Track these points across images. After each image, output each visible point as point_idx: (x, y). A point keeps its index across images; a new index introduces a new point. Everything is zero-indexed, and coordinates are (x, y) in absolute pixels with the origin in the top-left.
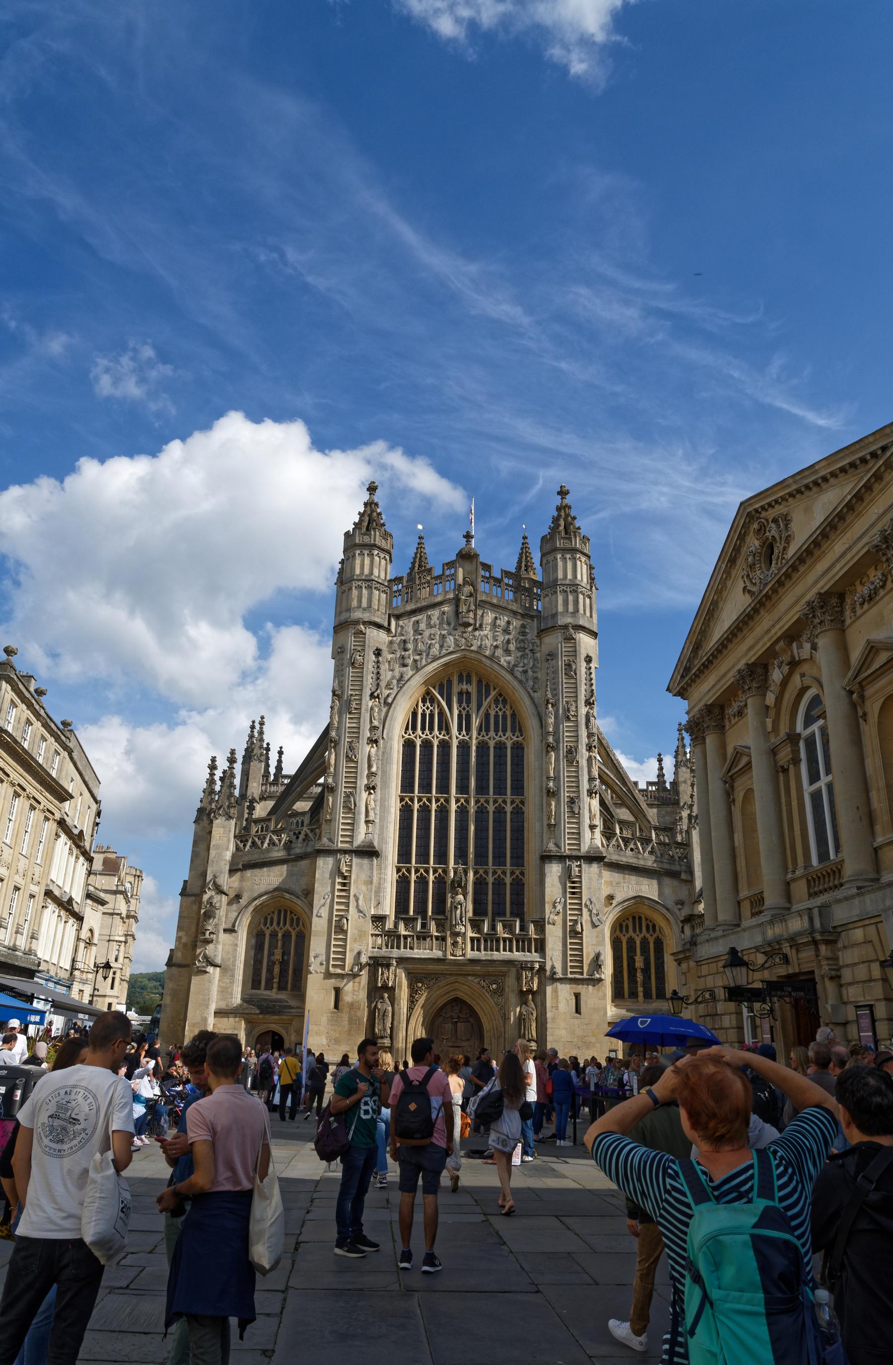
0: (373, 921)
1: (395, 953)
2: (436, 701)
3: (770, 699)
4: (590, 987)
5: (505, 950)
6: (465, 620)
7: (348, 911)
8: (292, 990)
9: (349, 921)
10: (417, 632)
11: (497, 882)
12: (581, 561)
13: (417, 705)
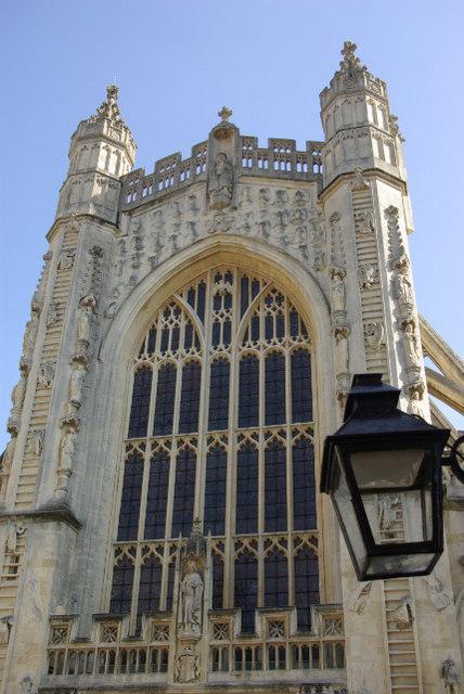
0: (54, 628)
5: (272, 667)
11: (273, 558)
12: (373, 105)
13: (157, 321)
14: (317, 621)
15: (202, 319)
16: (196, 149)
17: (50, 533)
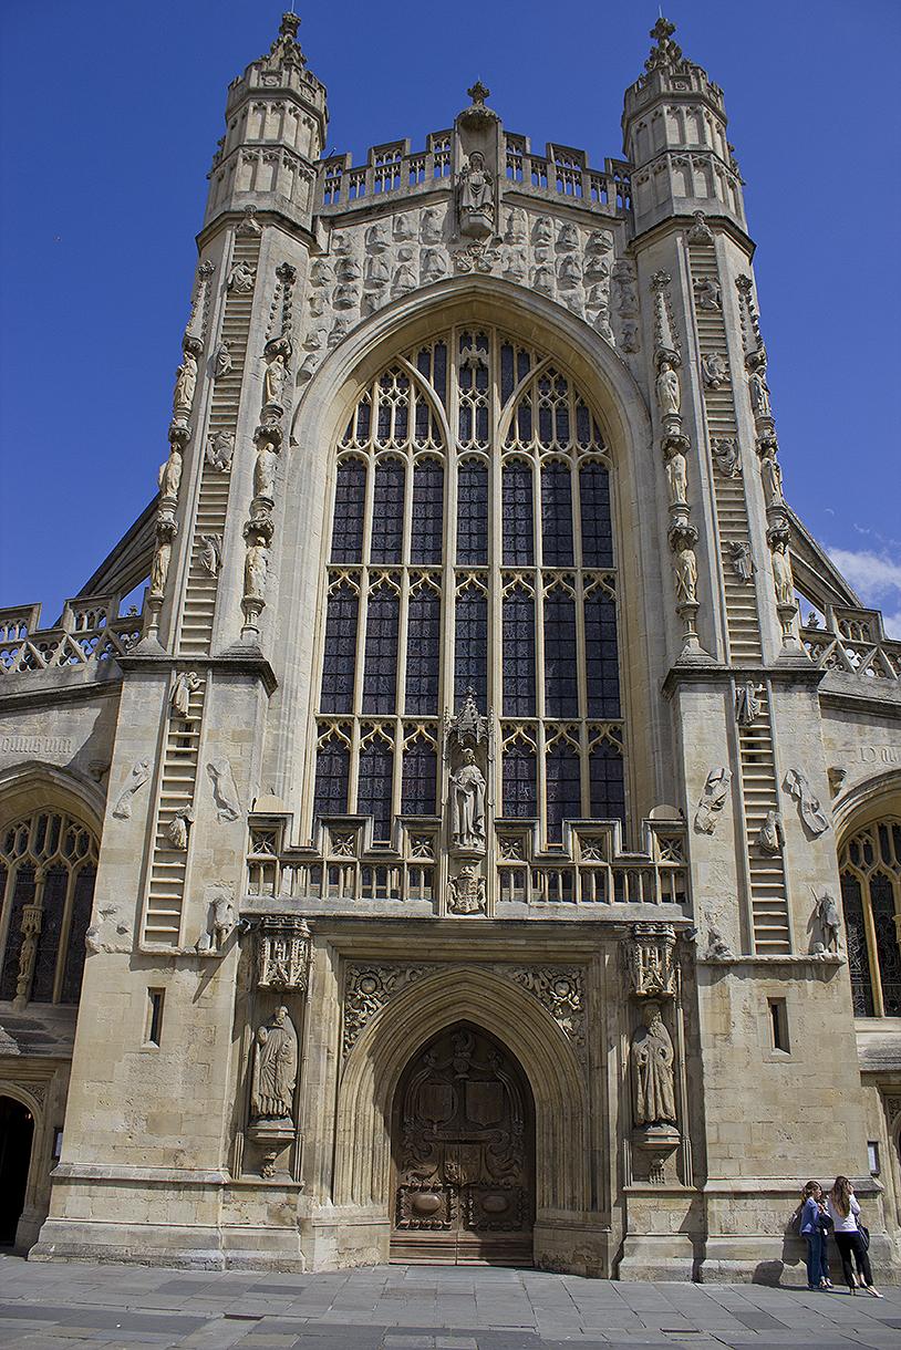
2: (412, 381)
4: (810, 984)
5: (586, 897)
6: (472, 219)
7: (191, 801)
8: (63, 1001)
9: (193, 828)
10: (376, 248)
11: (557, 754)
12: (709, 122)
15: (443, 402)
17: (240, 690)
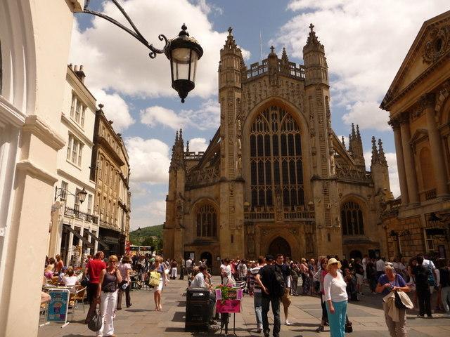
1: (255, 220)
3: (438, 108)
14: (308, 208)
16: (264, 61)
17: (240, 185)
